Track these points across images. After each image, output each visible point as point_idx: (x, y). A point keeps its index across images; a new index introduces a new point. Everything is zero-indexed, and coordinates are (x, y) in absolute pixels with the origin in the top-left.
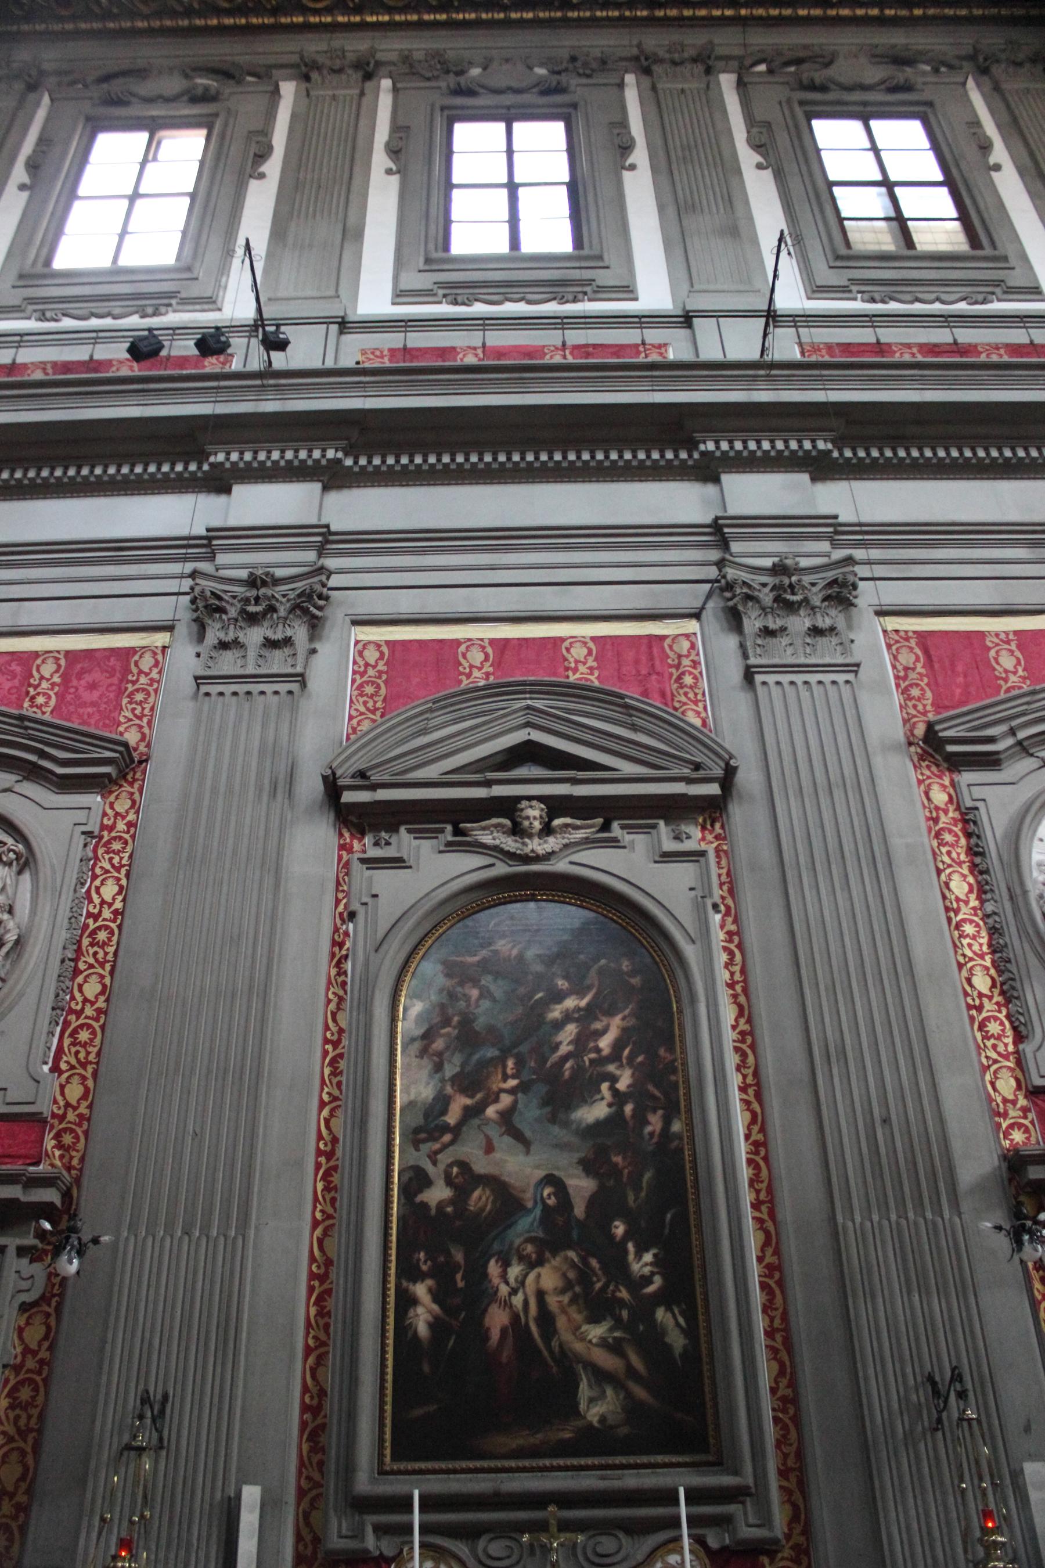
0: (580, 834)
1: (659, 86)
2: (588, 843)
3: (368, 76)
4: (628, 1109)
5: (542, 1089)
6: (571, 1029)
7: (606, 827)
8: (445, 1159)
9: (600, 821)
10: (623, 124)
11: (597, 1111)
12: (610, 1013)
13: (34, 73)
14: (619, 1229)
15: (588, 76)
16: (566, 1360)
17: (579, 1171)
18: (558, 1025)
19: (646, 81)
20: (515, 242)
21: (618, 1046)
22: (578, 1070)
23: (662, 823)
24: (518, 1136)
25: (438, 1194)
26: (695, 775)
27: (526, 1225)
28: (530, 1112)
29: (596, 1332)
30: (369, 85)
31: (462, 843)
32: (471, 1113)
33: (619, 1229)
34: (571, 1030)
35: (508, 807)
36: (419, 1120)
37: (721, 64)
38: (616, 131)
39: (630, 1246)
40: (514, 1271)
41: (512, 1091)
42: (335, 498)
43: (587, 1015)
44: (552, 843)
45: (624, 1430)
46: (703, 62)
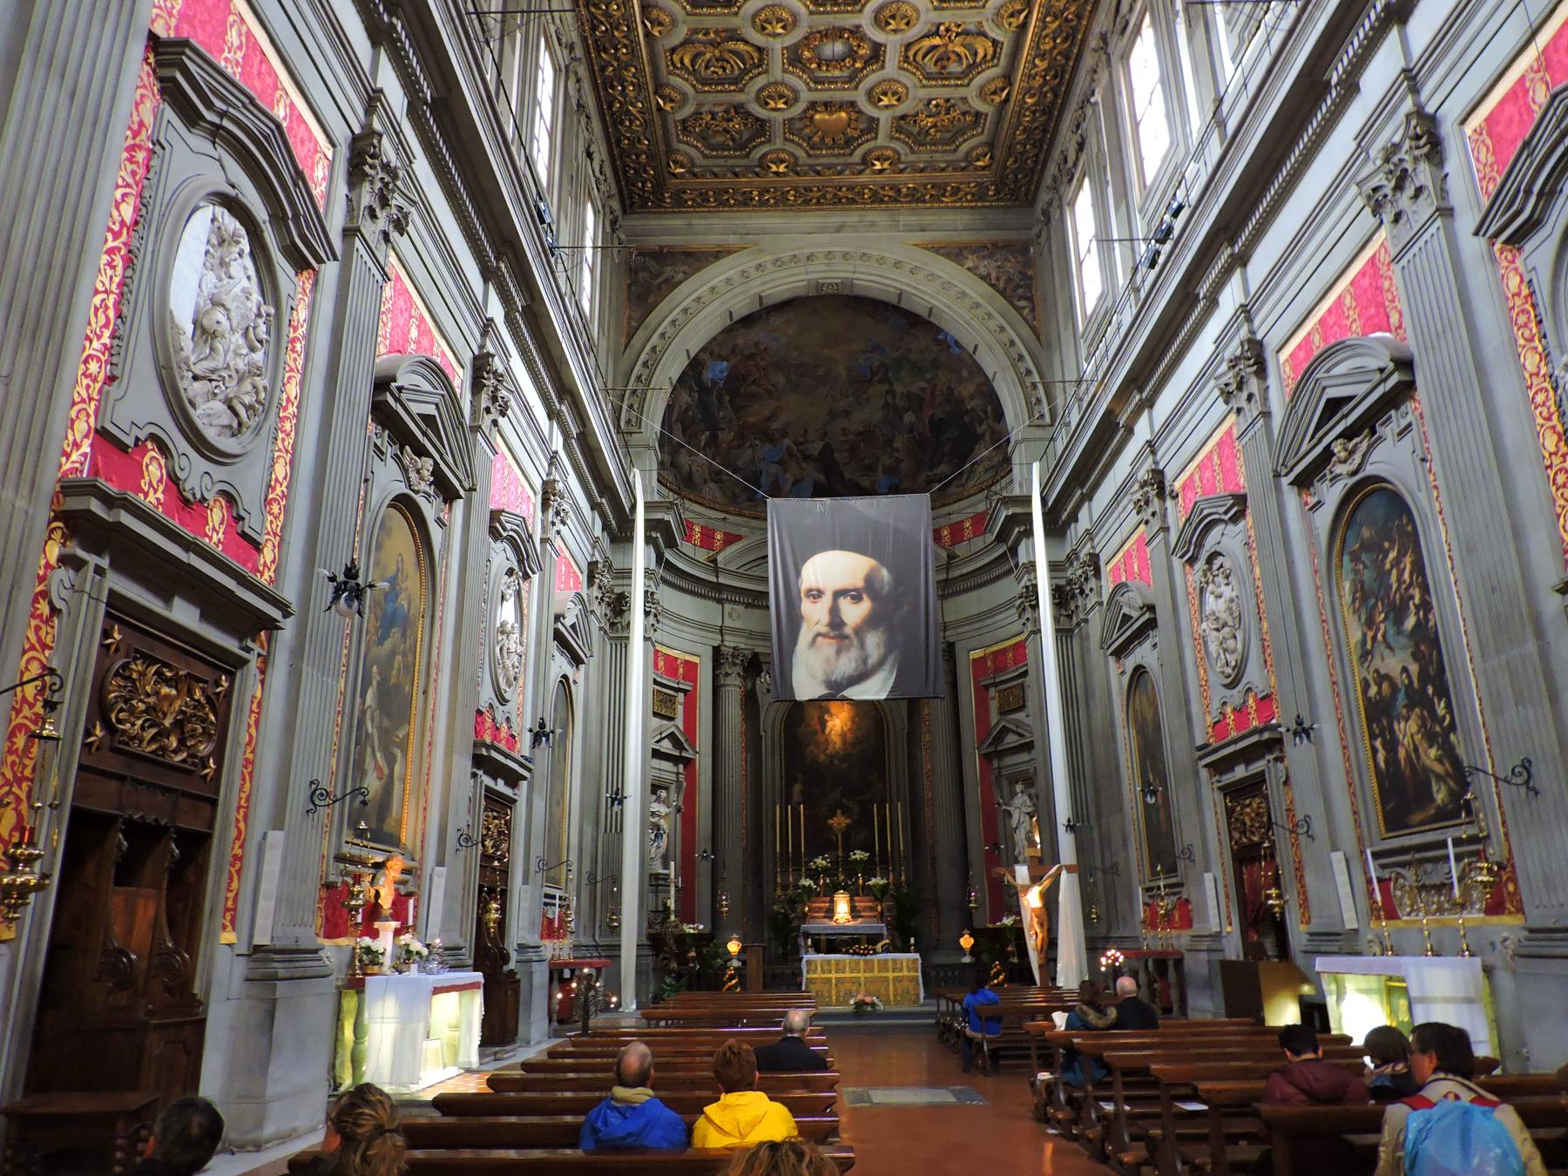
0: (1365, 445)
2: (1370, 448)
4: (1421, 613)
5: (1391, 615)
6: (1394, 572)
7: (1373, 432)
8: (1371, 670)
9: (1366, 431)
11: (1410, 622)
12: (1405, 555)
14: (1430, 690)
16: (1426, 770)
17: (1411, 660)
18: (1390, 572)
21: (1411, 576)
22: (1401, 596)
23: (1393, 412)
24: (1389, 647)
25: (1373, 690)
26: (1384, 375)
27: (1401, 699)
28: (1391, 631)
29: (1433, 752)
31: (1335, 479)
32: (1374, 638)
33: (1430, 690)
34: (1394, 572)
35: (1328, 454)
36: (1359, 652)
39: (1436, 700)
40: (1402, 725)
41: (1383, 621)
42: (1251, 267)
43: (1397, 562)
44: (1357, 458)
45: (1450, 807)
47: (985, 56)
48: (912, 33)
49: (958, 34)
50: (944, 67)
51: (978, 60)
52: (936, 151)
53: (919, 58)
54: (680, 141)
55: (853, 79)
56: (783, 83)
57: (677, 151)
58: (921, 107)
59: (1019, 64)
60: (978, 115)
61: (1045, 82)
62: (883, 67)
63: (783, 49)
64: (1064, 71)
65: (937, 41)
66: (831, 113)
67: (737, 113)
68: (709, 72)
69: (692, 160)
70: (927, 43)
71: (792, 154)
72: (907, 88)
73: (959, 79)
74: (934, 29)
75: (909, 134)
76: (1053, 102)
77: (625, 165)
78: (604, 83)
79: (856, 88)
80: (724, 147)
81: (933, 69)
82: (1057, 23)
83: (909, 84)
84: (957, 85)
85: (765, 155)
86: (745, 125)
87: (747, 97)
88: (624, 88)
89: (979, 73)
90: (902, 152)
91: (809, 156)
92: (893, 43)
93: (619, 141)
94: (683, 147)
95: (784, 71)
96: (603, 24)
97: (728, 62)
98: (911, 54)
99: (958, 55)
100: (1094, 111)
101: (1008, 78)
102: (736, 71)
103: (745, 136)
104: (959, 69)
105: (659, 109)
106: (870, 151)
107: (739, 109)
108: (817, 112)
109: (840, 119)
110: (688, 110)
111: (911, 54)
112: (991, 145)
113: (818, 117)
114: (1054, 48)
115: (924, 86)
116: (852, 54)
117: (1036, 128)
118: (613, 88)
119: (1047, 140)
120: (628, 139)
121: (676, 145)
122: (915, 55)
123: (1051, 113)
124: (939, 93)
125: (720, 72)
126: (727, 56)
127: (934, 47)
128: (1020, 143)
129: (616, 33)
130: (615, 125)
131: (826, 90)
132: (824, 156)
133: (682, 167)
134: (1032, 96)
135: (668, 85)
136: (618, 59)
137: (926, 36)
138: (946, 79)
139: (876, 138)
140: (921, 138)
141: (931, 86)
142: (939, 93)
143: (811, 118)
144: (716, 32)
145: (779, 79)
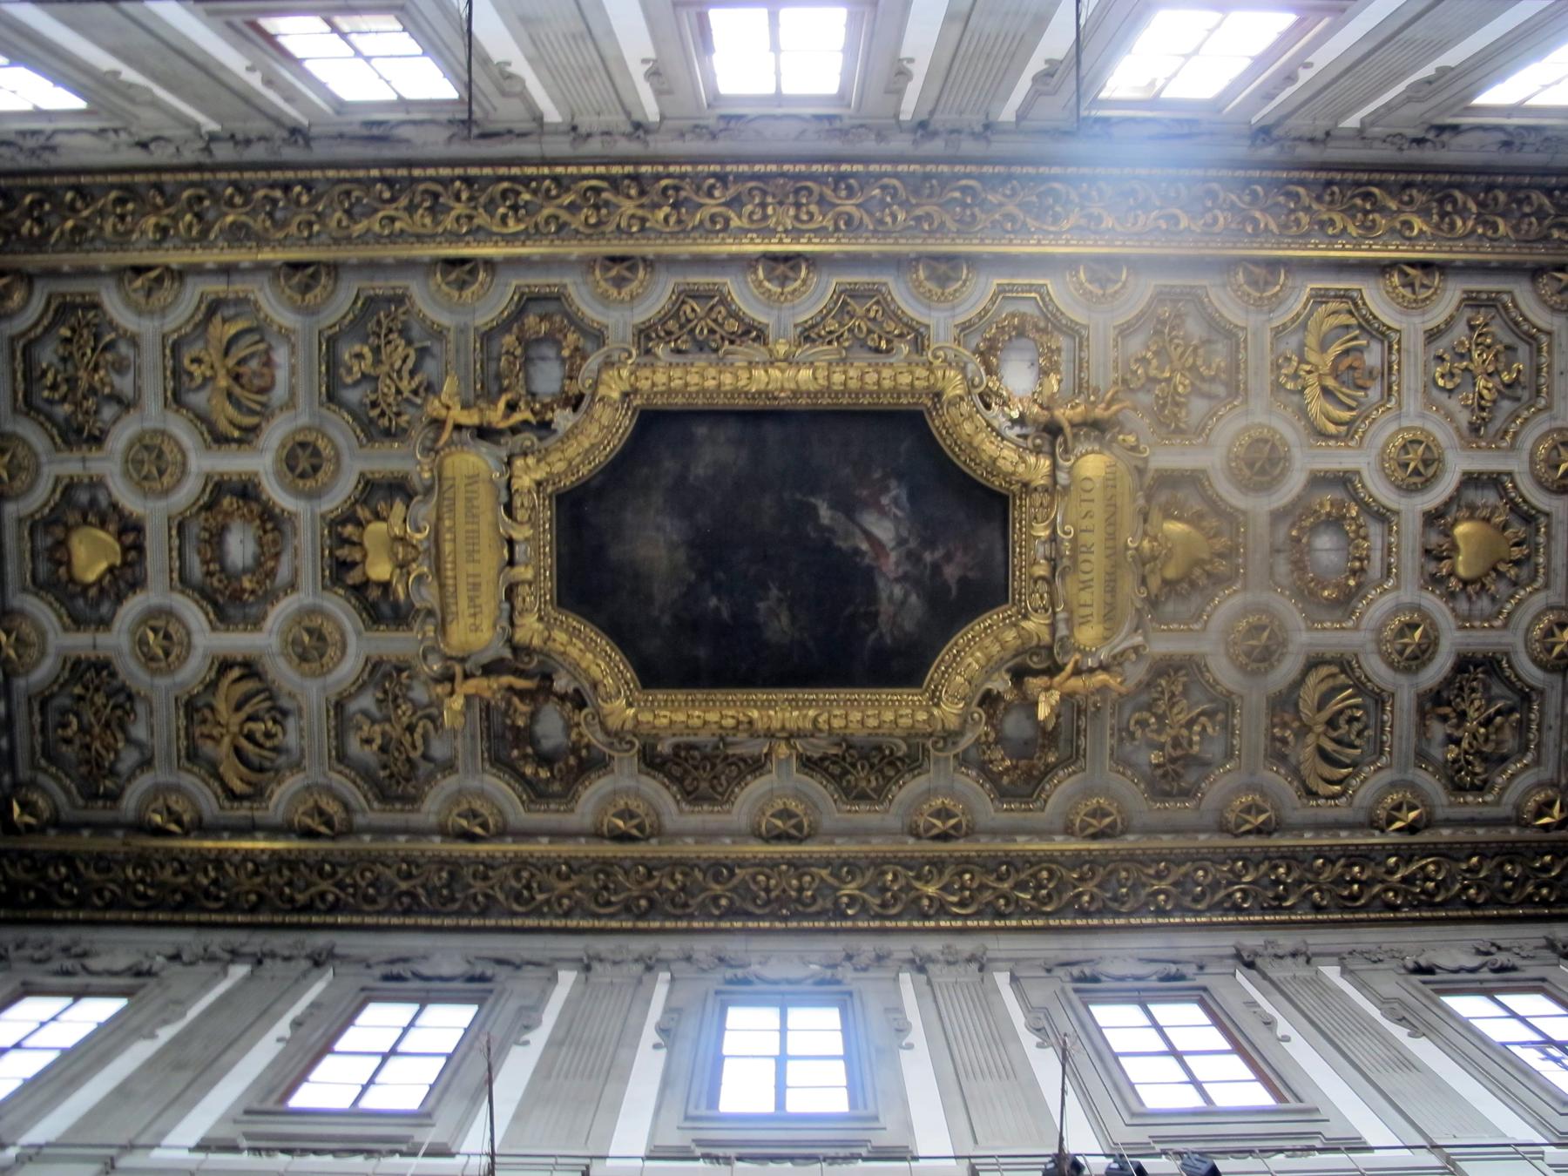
1: (623, 117)
3: (923, 125)
10: (659, 93)
13: (1259, 142)
15: (696, 126)
19: (637, 117)
20: (783, 1018)
30: (924, 116)
37: (562, 128)
38: (665, 87)
46: (580, 136)
47: (1350, 312)
48: (1287, 430)
49: (1302, 360)
50: (1371, 374)
51: (1353, 321)
52: (1550, 366)
53: (1346, 415)
54: (1497, 803)
55: (1383, 516)
56: (1379, 630)
57: (1518, 807)
58: (1454, 404)
59: (1347, 259)
60: (1472, 301)
61: (1382, 210)
62: (1358, 473)
63: (1309, 629)
64: (1358, 184)
65: (1313, 392)
66: (1455, 548)
67: (1449, 704)
68: (1357, 742)
69: (1541, 785)
70: (1316, 405)
71: (1537, 618)
72: (1401, 430)
73: (1390, 347)
74: (1296, 398)
75: (1514, 416)
76: (1423, 186)
77: (1528, 901)
78: (1344, 909)
79: (1397, 513)
80: (1522, 727)
81: (1375, 393)
82: (1258, 215)
83: (1393, 427)
84: (1399, 351)
85: (1535, 661)
86: (1473, 690)
87: (1406, 691)
88: (1354, 880)
89: (1375, 318)
90: (1545, 427)
91: (1547, 586)
92: (1305, 461)
93: (1471, 904)
94: (1511, 796)
95: (1356, 628)
96: (1230, 895)
97: (1341, 712)
98: (1332, 428)
99: (1346, 352)
100: (1373, 124)
101: (1383, 268)
102: (1358, 700)
103: (1497, 689)
104: (1376, 347)
105: (1412, 829)
106: (1540, 483)
107: (1434, 702)
108: (1452, 573)
109: (1466, 536)
110: (1431, 784)
111: (1332, 428)
112: (1535, 272)
113: (1461, 571)
114: (1308, 209)
115: (1399, 404)
116: (1335, 522)
117: (1481, 204)
118: (1354, 897)
119: (1511, 179)
120: (1465, 888)
121: (1506, 810)
122: (1337, 423)
123: (1451, 185)
124: (1411, 377)
125: (1357, 726)
126: (1326, 714)
127: (1326, 392)
128: (1516, 229)
129: (1247, 879)
130: (1433, 906)
131: (1399, 560)
132: (1549, 560)
133: (1549, 804)
134: (1408, 225)
135: (1371, 810)
136: (1299, 883)
137: (1303, 412)
138: (1390, 368)
139: (1510, 474)
140: (1525, 395)
141: (1399, 391)
142: (1411, 377)
143: (1466, 583)
144: (1285, 726)
145: (1369, 636)
